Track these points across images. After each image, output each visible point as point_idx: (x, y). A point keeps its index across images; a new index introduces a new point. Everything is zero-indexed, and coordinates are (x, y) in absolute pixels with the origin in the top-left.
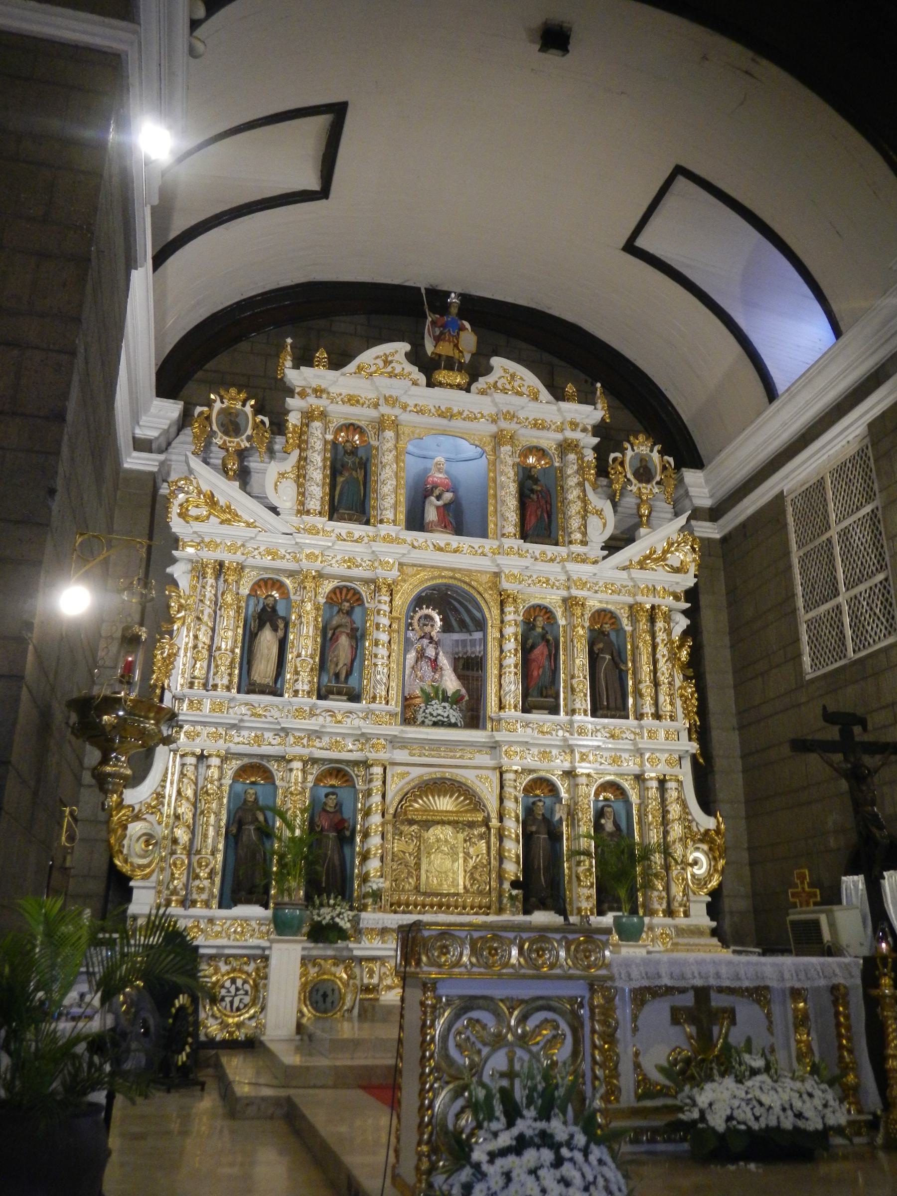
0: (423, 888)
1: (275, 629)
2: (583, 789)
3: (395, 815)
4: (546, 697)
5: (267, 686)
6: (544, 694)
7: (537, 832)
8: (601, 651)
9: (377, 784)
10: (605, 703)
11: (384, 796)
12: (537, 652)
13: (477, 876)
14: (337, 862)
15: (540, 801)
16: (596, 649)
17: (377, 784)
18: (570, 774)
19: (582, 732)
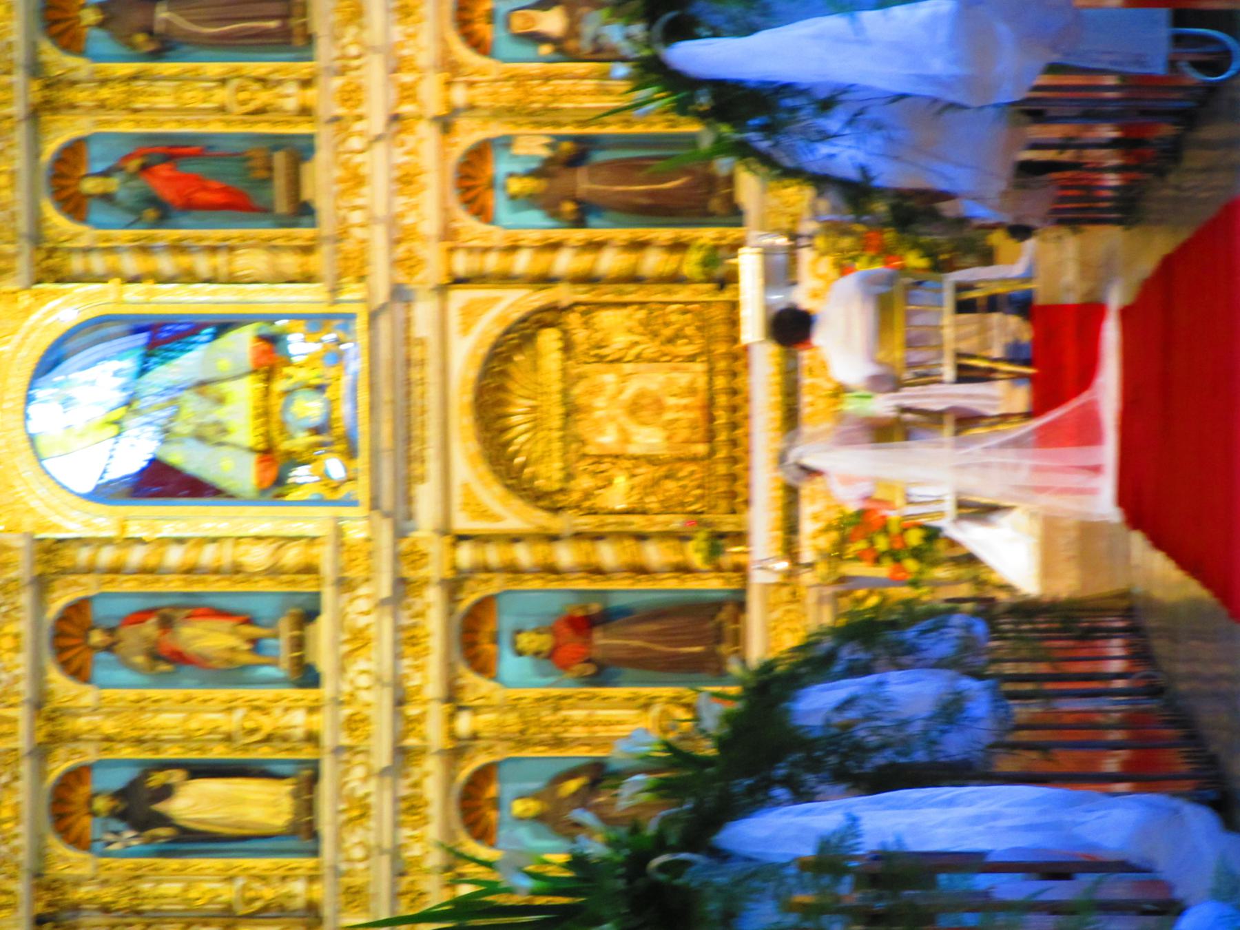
0: (701, 449)
1: (166, 792)
2: (480, 96)
3: (556, 510)
4: (270, 169)
5: (295, 795)
6: (262, 174)
7: (578, 202)
8: (150, 32)
9: (493, 555)
10: (273, 24)
11: (515, 539)
12: (168, 193)
13: (667, 332)
14: (653, 627)
15: (505, 187)
16: (151, 47)
17: (493, 555)
18: (445, 124)
19: (352, 96)
